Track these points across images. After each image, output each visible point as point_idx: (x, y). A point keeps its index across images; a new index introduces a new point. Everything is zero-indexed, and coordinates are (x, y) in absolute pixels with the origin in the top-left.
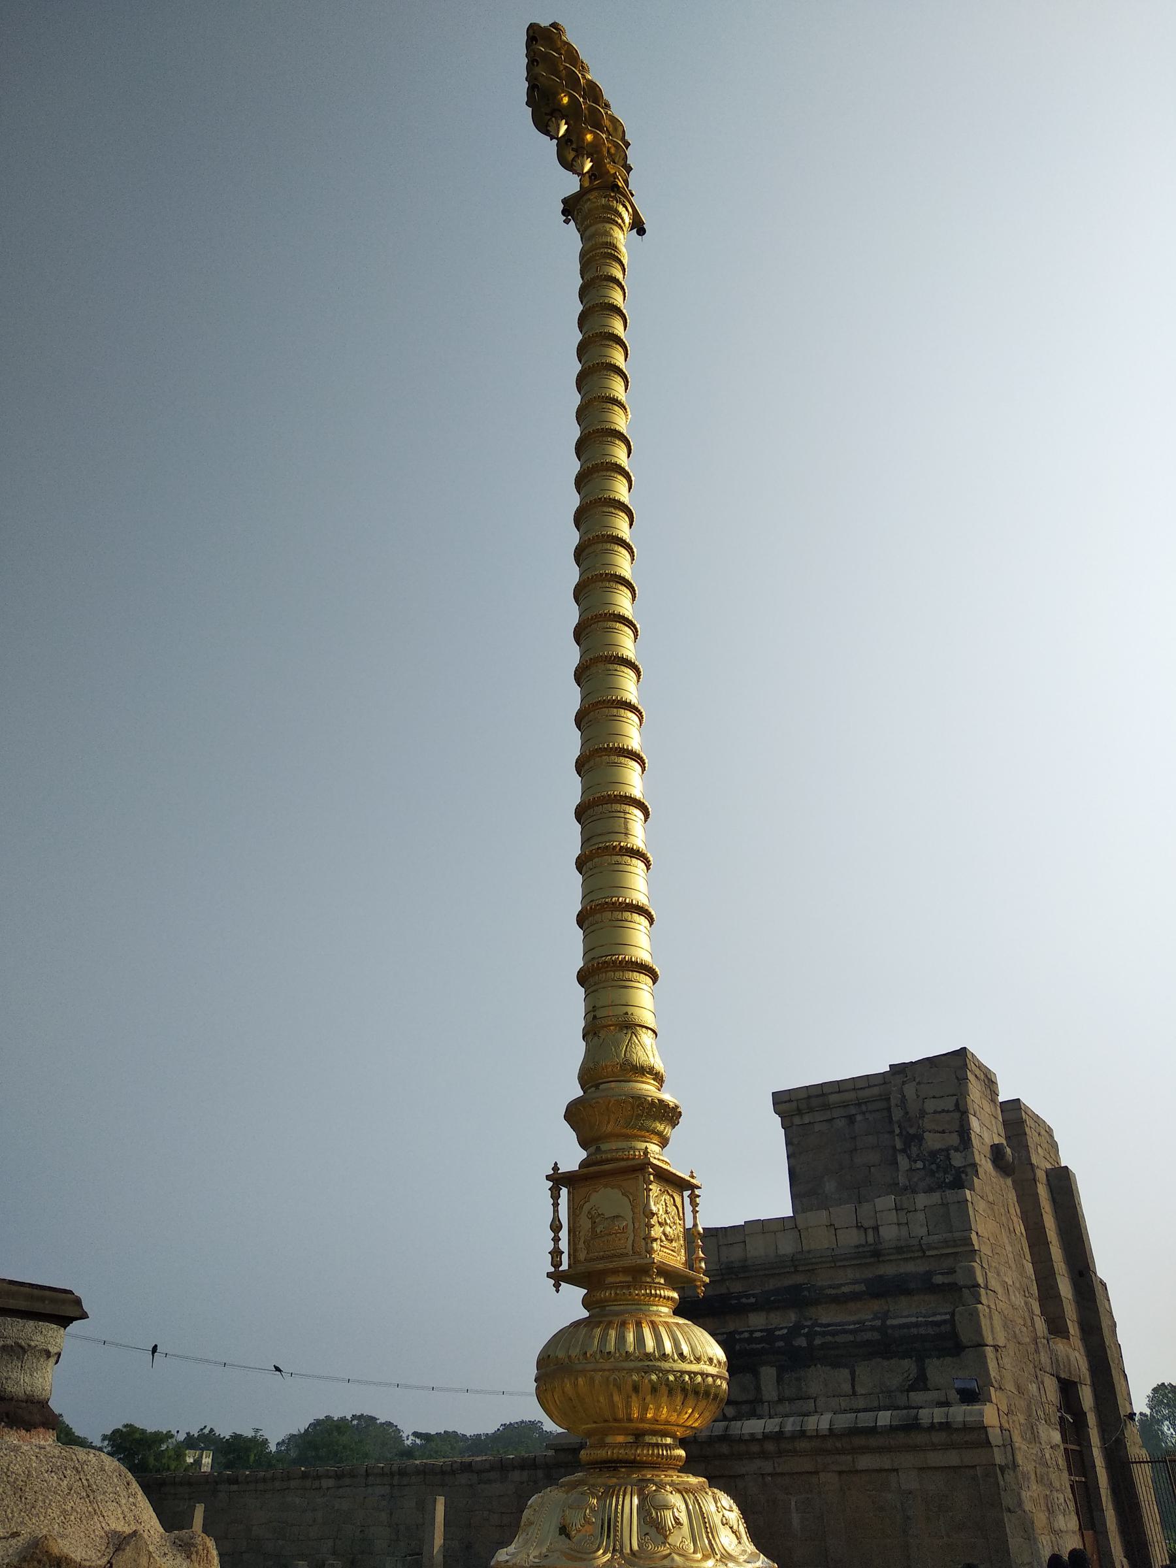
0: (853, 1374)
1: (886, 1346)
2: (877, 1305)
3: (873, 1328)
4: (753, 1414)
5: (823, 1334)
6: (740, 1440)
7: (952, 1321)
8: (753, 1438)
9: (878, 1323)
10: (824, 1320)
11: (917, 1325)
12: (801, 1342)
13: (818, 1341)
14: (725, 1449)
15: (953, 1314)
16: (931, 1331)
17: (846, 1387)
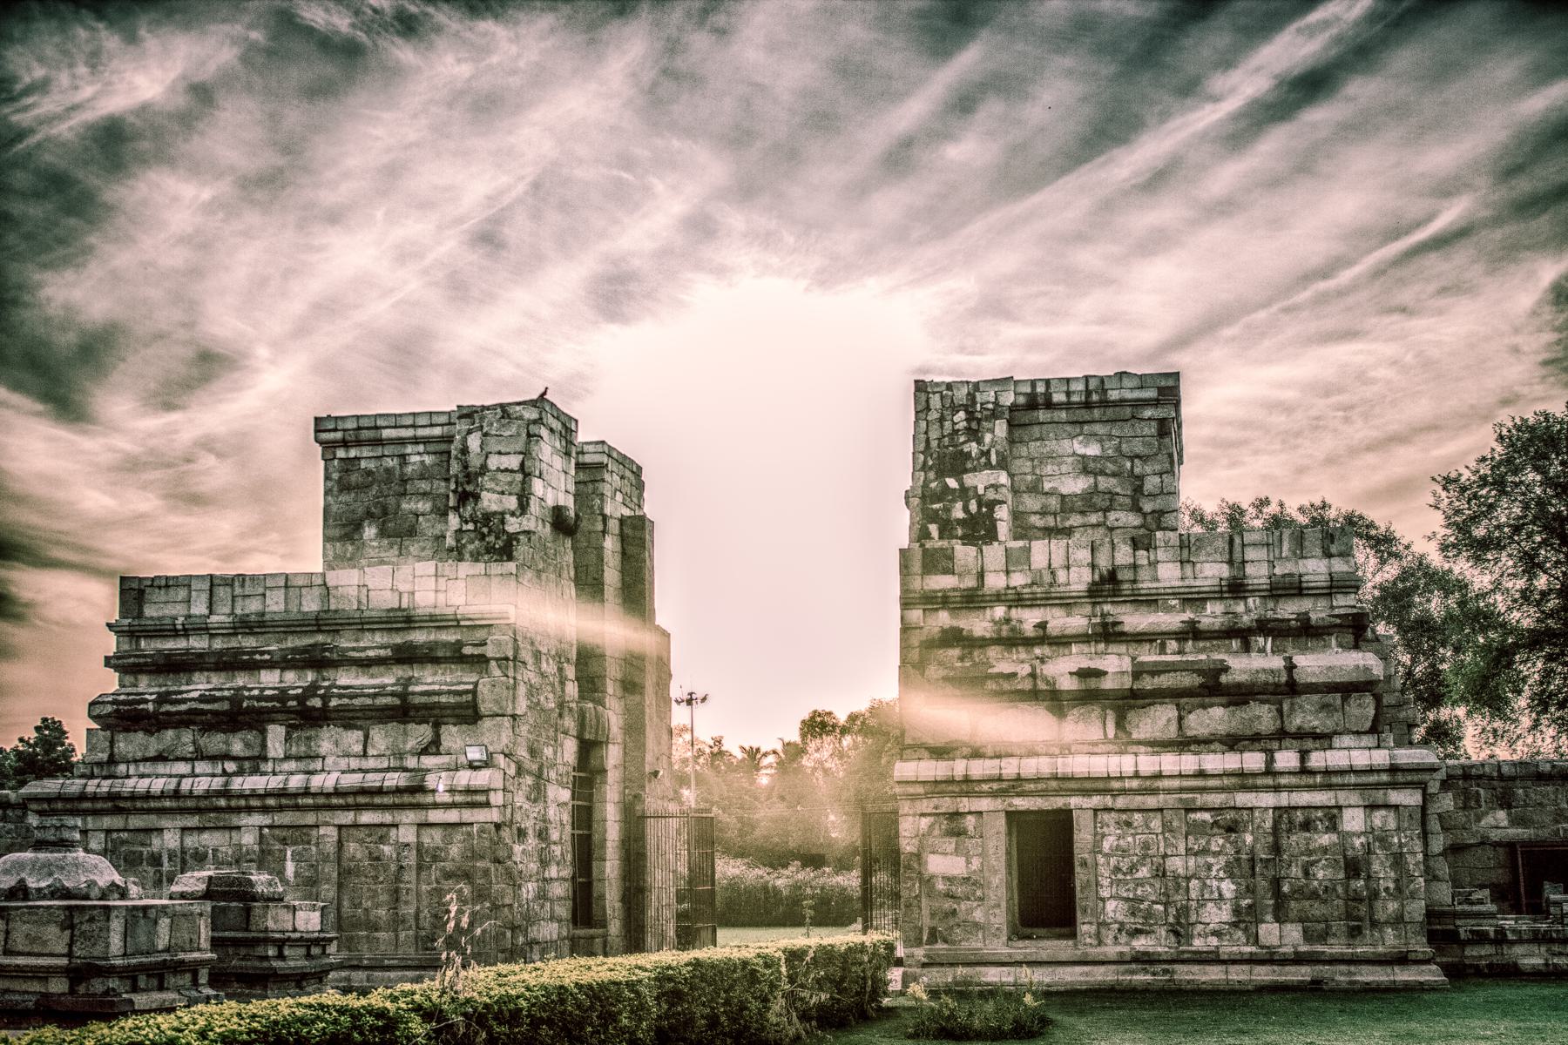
0: (367, 737)
1: (403, 711)
2: (400, 672)
3: (393, 694)
4: (255, 771)
5: (340, 696)
6: (241, 796)
7: (474, 692)
8: (254, 794)
9: (399, 689)
11: (439, 693)
12: (316, 702)
13: (334, 703)
14: (222, 802)
15: (476, 684)
16: (452, 700)
17: (358, 748)
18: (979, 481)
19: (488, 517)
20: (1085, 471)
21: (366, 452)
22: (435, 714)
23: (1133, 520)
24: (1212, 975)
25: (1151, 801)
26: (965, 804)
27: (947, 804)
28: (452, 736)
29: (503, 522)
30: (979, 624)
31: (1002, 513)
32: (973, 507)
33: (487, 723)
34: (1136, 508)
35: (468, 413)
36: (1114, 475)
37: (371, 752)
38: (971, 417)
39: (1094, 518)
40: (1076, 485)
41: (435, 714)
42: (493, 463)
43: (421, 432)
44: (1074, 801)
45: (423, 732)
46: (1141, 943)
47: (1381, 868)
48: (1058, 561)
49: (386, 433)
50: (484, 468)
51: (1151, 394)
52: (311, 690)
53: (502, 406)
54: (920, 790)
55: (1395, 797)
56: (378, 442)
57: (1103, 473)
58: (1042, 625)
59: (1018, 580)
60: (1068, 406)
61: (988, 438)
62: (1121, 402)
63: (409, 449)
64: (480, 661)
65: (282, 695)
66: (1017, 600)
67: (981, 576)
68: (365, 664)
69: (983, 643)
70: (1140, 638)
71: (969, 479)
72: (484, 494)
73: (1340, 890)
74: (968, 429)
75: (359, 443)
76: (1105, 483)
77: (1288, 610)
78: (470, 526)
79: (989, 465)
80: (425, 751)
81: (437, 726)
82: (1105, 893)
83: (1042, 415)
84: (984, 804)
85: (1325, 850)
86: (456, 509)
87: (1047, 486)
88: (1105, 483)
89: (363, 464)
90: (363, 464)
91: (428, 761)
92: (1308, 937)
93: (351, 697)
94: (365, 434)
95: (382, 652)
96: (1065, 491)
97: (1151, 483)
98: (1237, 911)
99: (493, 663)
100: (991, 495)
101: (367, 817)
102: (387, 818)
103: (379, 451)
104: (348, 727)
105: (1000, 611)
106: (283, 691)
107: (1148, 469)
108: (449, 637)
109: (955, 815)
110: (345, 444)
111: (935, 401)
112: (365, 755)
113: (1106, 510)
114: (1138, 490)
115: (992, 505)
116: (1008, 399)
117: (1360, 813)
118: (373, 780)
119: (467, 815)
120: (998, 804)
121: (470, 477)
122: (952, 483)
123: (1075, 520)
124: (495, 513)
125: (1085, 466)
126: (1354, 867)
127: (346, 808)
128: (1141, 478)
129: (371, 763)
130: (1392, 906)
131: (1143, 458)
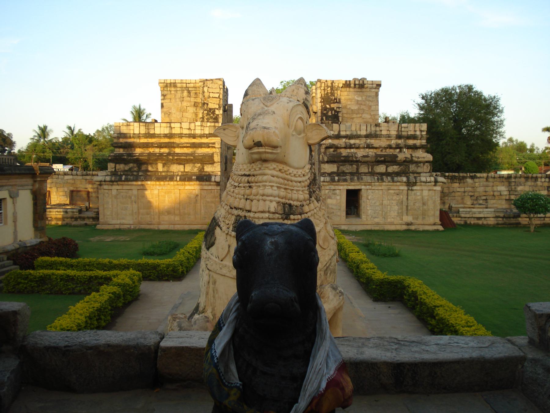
19: (210, 109)
23: (368, 116)
24: (392, 228)
25: (380, 188)
32: (333, 113)
36: (365, 105)
38: (332, 89)
39: (359, 116)
44: (363, 187)
46: (376, 220)
47: (430, 203)
53: (212, 80)
55: (435, 188)
57: (362, 104)
61: (336, 95)
67: (339, 131)
70: (376, 148)
73: (421, 209)
76: (362, 107)
77: (411, 142)
82: (368, 208)
85: (418, 199)
87: (348, 107)
88: (362, 107)
92: (413, 219)
97: (373, 108)
98: (398, 213)
100: (338, 110)
107: (373, 104)
111: (323, 85)
113: (362, 114)
116: (341, 85)
117: (427, 191)
122: (328, 106)
123: (355, 116)
124: (212, 109)
126: (424, 204)
127: (182, 185)
128: (371, 106)
130: (432, 212)
131: (372, 101)
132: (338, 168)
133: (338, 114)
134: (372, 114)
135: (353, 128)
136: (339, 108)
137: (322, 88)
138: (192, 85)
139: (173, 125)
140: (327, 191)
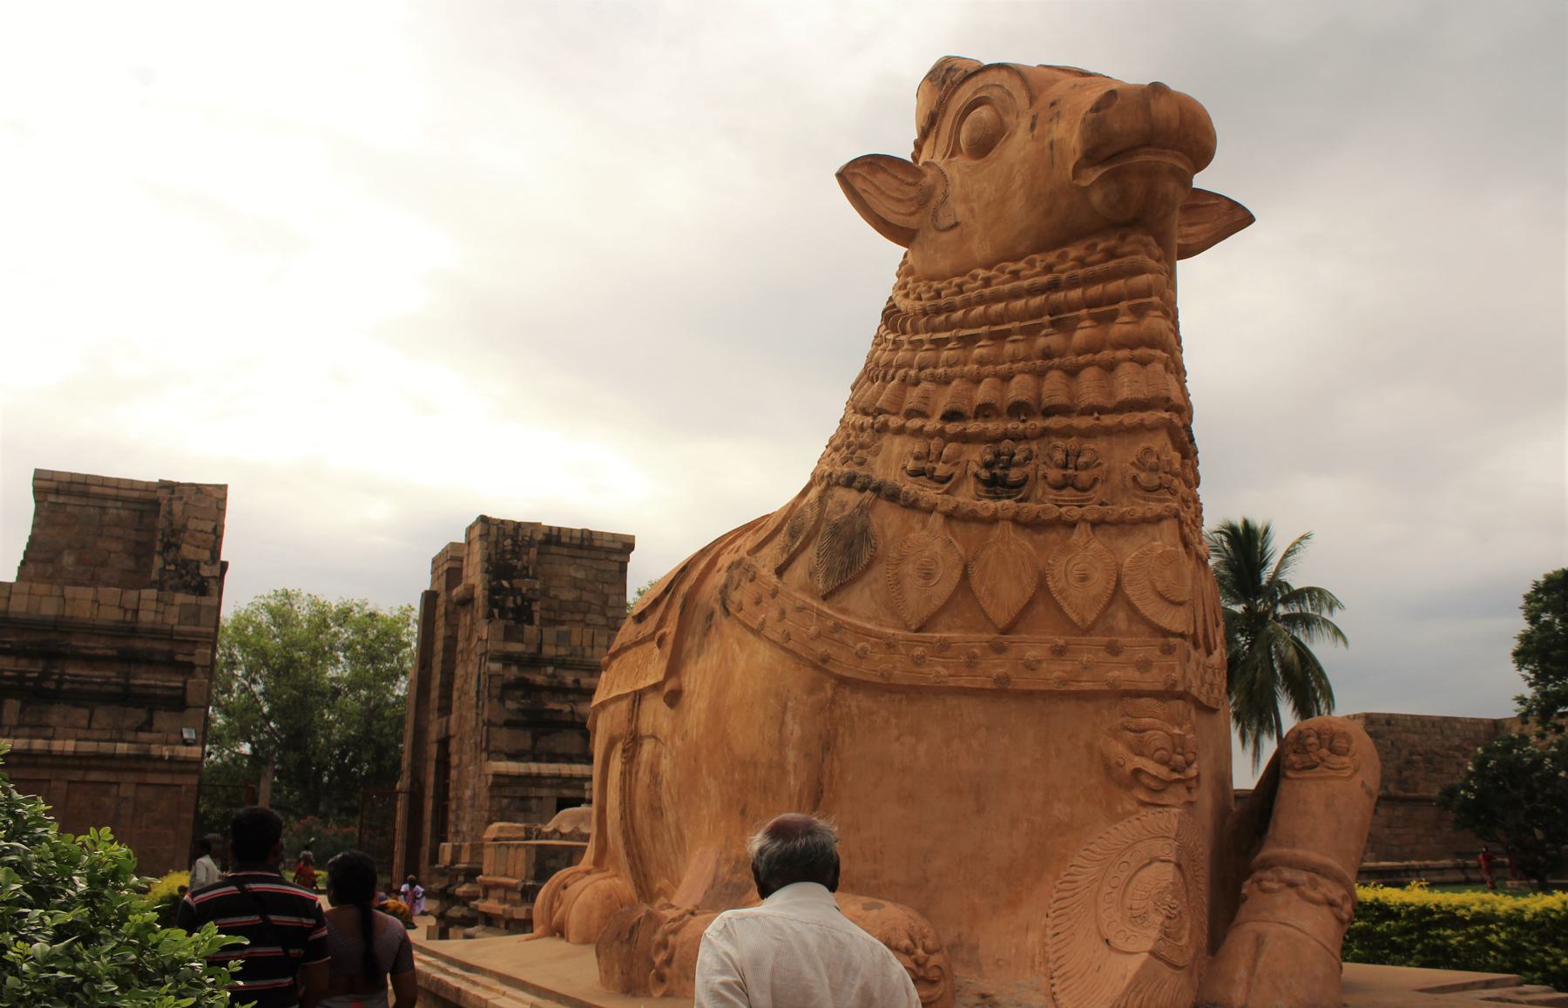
0: (92, 714)
1: (125, 697)
3: (117, 684)
5: (73, 682)
7: (184, 689)
9: (122, 680)
10: (71, 671)
12: (51, 685)
13: (66, 686)
15: (185, 683)
16: (165, 692)
17: (84, 722)
18: (524, 585)
19: (186, 563)
20: (575, 587)
21: (73, 500)
22: (152, 702)
23: (601, 620)
26: (533, 792)
27: (520, 792)
28: (163, 720)
29: (198, 567)
30: (539, 679)
31: (536, 607)
32: (519, 601)
33: (191, 712)
34: (604, 615)
35: (169, 487)
37: (94, 725)
38: (515, 543)
39: (578, 617)
40: (569, 595)
41: (152, 702)
42: (192, 524)
43: (123, 493)
45: (140, 715)
48: (587, 640)
49: (94, 489)
50: (184, 528)
51: (619, 546)
52: (45, 676)
54: (507, 781)
56: (85, 495)
58: (577, 681)
59: (562, 651)
60: (569, 546)
61: (525, 558)
62: (601, 549)
63: (109, 504)
64: (188, 668)
65: (21, 677)
66: (561, 664)
68: (91, 660)
69: (539, 689)
71: (516, 582)
72: (184, 546)
74: (512, 551)
75: (69, 493)
76: (586, 596)
78: (172, 567)
79: (527, 576)
80: (140, 729)
81: (151, 712)
83: (553, 549)
84: (544, 792)
86: (161, 553)
87: (552, 593)
89: (69, 509)
90: (69, 509)
91: (144, 736)
93: (81, 683)
94: (75, 487)
95: (110, 652)
96: (562, 597)
97: (613, 600)
99: (198, 670)
100: (530, 595)
101: (94, 776)
102: (112, 777)
103: (84, 501)
104: (77, 705)
105: (550, 670)
106: (21, 673)
108: (164, 646)
109: (525, 799)
110: (57, 492)
111: (494, 530)
112: (89, 727)
114: (605, 603)
115: (531, 601)
116: (539, 537)
118: (106, 747)
119: (178, 780)
120: (554, 793)
121: (174, 533)
122: (505, 584)
123: (567, 616)
125: (575, 584)
127: (79, 768)
129: (97, 735)
132: (535, 739)
133: (530, 605)
134: (610, 614)
135: (576, 640)
136: (534, 590)
137: (492, 539)
138: (136, 494)
139: (70, 591)
140: (505, 801)
